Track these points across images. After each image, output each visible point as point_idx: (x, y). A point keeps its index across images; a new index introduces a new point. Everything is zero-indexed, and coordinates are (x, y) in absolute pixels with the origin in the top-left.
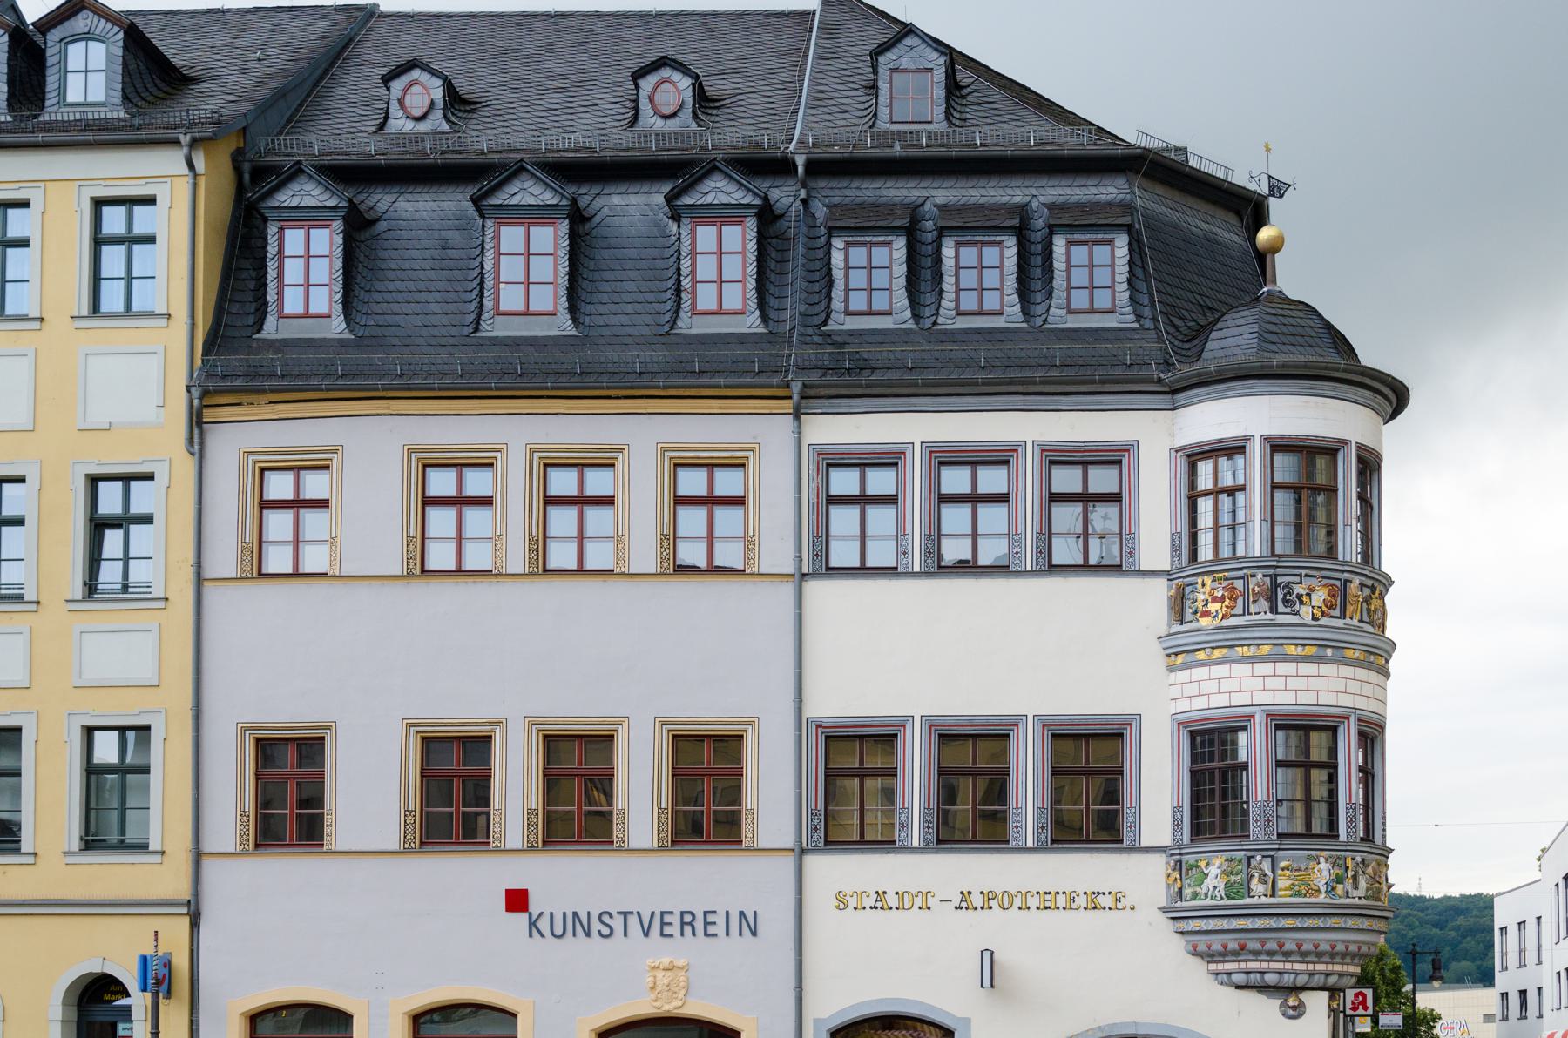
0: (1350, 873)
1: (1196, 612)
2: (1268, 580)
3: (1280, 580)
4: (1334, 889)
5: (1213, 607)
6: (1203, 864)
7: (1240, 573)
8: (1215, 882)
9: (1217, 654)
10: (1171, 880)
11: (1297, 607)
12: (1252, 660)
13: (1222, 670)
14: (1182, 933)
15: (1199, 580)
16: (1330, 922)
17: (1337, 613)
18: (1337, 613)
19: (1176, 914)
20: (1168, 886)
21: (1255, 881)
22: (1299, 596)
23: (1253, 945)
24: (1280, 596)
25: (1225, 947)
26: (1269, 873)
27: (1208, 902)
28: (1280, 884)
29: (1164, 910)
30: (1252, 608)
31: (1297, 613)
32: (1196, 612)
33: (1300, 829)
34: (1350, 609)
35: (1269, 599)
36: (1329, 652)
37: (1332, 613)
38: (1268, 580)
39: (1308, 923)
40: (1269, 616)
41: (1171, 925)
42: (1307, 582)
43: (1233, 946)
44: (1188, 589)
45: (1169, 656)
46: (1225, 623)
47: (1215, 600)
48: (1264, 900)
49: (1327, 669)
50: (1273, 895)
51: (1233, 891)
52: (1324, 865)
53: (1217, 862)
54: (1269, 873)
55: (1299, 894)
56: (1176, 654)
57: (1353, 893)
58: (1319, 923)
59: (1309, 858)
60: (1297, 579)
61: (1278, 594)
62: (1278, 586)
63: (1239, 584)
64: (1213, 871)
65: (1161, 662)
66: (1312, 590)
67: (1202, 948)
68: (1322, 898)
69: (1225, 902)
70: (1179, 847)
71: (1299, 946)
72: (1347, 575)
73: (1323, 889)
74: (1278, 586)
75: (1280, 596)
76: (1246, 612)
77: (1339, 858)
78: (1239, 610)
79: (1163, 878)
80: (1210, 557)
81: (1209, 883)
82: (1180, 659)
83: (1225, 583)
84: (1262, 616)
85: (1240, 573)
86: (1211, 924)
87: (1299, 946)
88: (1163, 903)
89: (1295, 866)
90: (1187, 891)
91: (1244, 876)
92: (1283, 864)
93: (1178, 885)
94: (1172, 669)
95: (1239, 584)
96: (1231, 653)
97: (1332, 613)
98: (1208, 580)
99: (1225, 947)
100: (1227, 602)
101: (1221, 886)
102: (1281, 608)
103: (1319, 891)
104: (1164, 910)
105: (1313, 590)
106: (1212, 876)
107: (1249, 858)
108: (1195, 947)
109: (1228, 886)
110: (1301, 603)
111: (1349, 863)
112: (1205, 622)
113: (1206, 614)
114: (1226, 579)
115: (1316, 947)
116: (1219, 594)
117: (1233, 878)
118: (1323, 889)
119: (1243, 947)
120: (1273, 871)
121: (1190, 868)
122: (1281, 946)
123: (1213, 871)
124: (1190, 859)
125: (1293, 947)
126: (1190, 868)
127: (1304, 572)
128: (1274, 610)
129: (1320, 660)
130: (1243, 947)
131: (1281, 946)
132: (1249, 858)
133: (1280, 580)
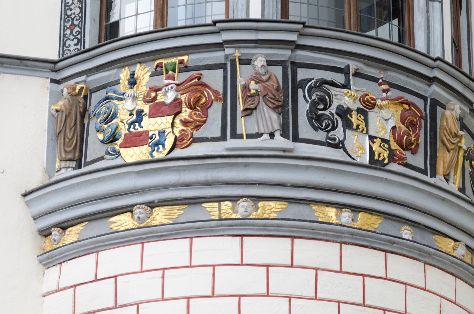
1: (113, 139)
2: (277, 71)
3: (302, 74)
5: (151, 125)
7: (217, 56)
9: (160, 216)
11: (339, 133)
12: (241, 229)
13: (163, 252)
15: (124, 75)
17: (418, 160)
18: (418, 160)
22: (344, 113)
24: (304, 107)
30: (243, 126)
31: (338, 145)
32: (113, 139)
34: (444, 158)
35: (280, 109)
36: (407, 233)
37: (410, 158)
38: (277, 71)
40: (280, 142)
42: (359, 87)
44: (96, 97)
45: (45, 233)
46: (177, 153)
47: (158, 110)
49: (402, 267)
56: (64, 226)
60: (339, 78)
61: (302, 102)
62: (297, 85)
63: (214, 79)
65: (27, 245)
66: (367, 106)
72: (436, 90)
74: (298, 85)
75: (304, 107)
76: (229, 130)
78: (213, 127)
80: (146, 23)
82: (72, 234)
83: (182, 77)
84: (264, 142)
85: (217, 56)
94: (50, 260)
95: (214, 79)
96: (194, 213)
97: (410, 158)
98: (143, 72)
100: (186, 114)
102: (305, 130)
105: (372, 105)
110: (348, 125)
112: (131, 154)
113: (135, 140)
114: (186, 69)
116: (169, 97)
127: (353, 65)
128: (289, 130)
129: (388, 246)
133: (302, 74)
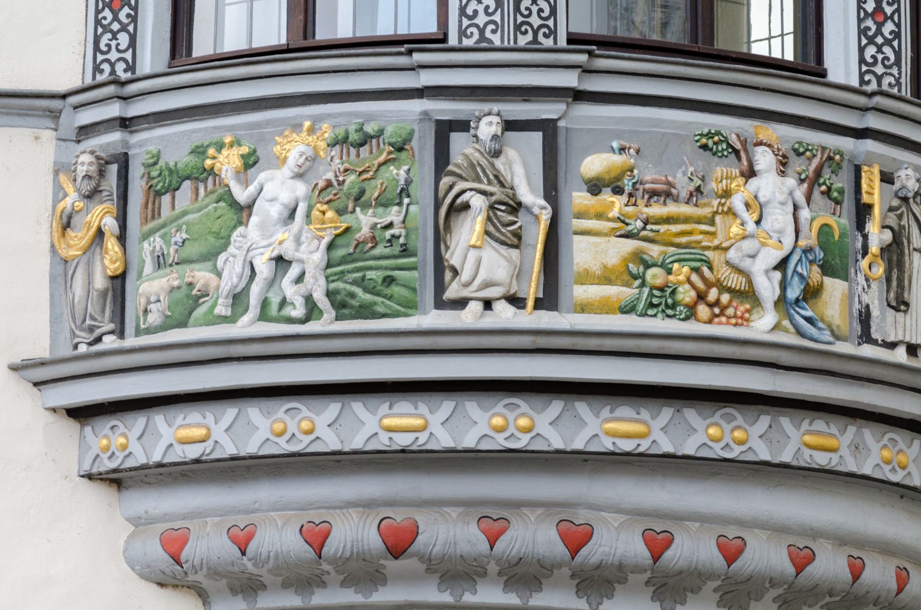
0: (878, 237)
4: (811, 293)
6: (227, 163)
8: (284, 240)
10: (79, 237)
14: (116, 480)
16: (796, 440)
19: (96, 395)
20: (63, 270)
21: (469, 230)
23: (449, 533)
25: (317, 539)
26: (530, 194)
27: (247, 326)
28: (586, 252)
29: (38, 374)
33: (676, 35)
39: (704, 433)
41: (70, 447)
43: (354, 533)
48: (505, 315)
50: (549, 299)
51: (362, 276)
52: (771, 185)
53: (295, 150)
54: (530, 194)
55: (663, 301)
57: (887, 324)
58: (751, 436)
59: (711, 146)
64: (277, 188)
67: (209, 545)
68: (763, 325)
69: (326, 323)
70: (121, 87)
71: (658, 545)
73: (767, 287)
77: (831, 160)
79: (41, 234)
81: (257, 241)
86: (262, 429)
87: (658, 545)
88: (38, 344)
89: (650, 175)
90: (151, 289)
91: (421, 210)
92: (595, 164)
93: (111, 258)
99: (317, 539)
101: (312, 256)
103: (748, 295)
104: (38, 374)
106: (268, 210)
107: (445, 129)
108: (174, 546)
109: (342, 253)
111: (874, 193)
115: (731, 553)
117: (365, 221)
118: (767, 287)
119: (399, 544)
120: (551, 191)
121: (167, 183)
122: (576, 540)
123: (277, 188)
124: (170, 144)
125: (633, 547)
126: (167, 183)
130: (399, 544)
131: (576, 540)
132: (445, 129)
